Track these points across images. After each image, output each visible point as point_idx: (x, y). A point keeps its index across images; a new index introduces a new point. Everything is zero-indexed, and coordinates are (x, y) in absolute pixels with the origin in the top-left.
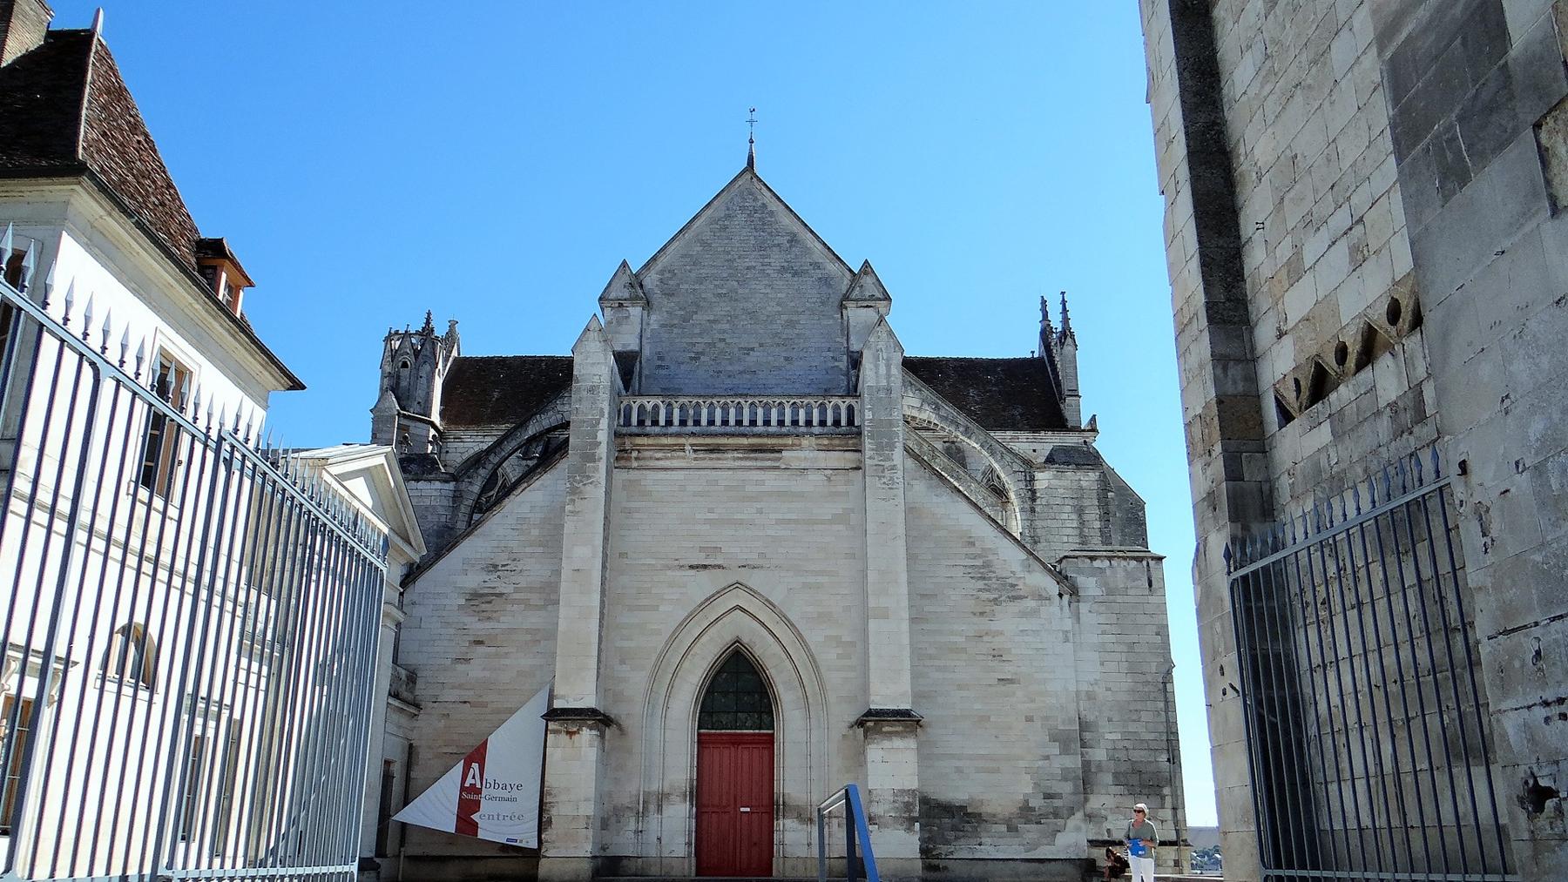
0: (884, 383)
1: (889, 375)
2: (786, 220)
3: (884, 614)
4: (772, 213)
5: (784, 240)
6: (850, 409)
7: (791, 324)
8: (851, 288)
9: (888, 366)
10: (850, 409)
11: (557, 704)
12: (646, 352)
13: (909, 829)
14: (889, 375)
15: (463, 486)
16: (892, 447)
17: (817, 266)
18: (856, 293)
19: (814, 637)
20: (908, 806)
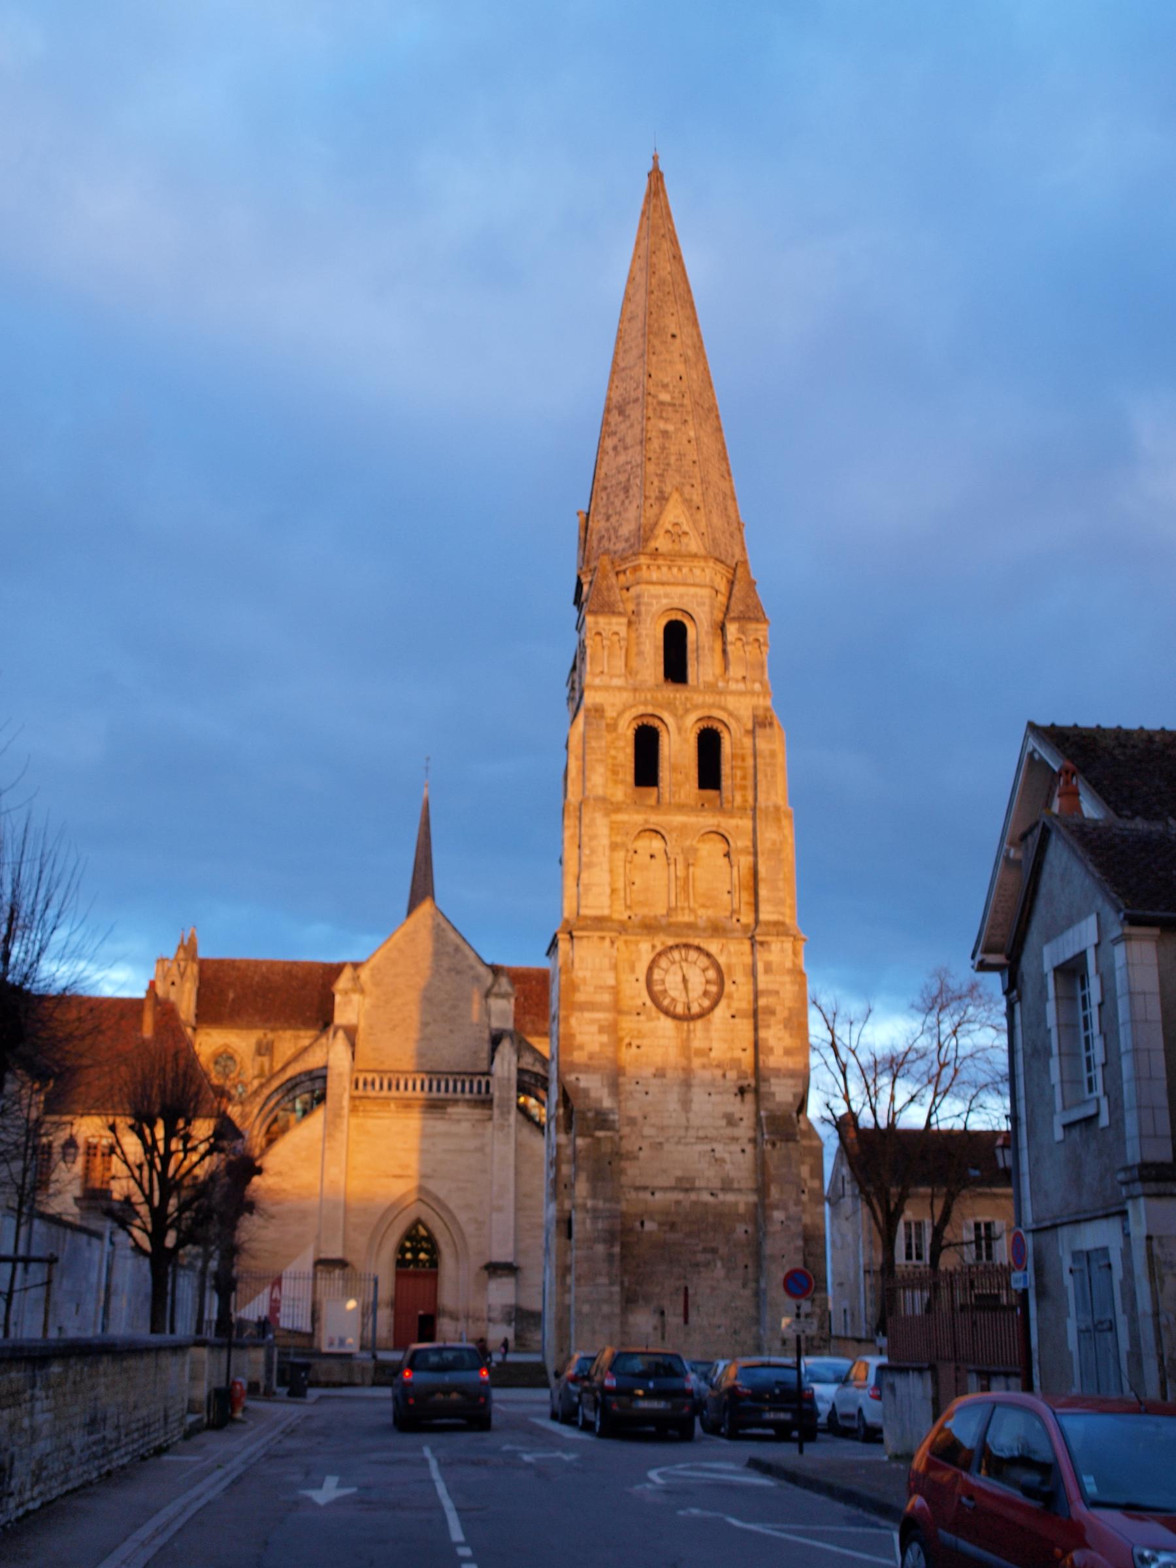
0: (506, 1075)
1: (509, 1070)
2: (452, 935)
3: (500, 1209)
4: (443, 930)
5: (451, 949)
6: (488, 1084)
7: (454, 1007)
8: (493, 986)
9: (509, 1064)
10: (488, 1084)
11: (323, 1256)
12: (362, 1025)
13: (509, 1324)
14: (509, 1070)
15: (247, 1109)
16: (509, 1113)
17: (472, 967)
18: (496, 989)
19: (462, 1217)
20: (509, 1313)
